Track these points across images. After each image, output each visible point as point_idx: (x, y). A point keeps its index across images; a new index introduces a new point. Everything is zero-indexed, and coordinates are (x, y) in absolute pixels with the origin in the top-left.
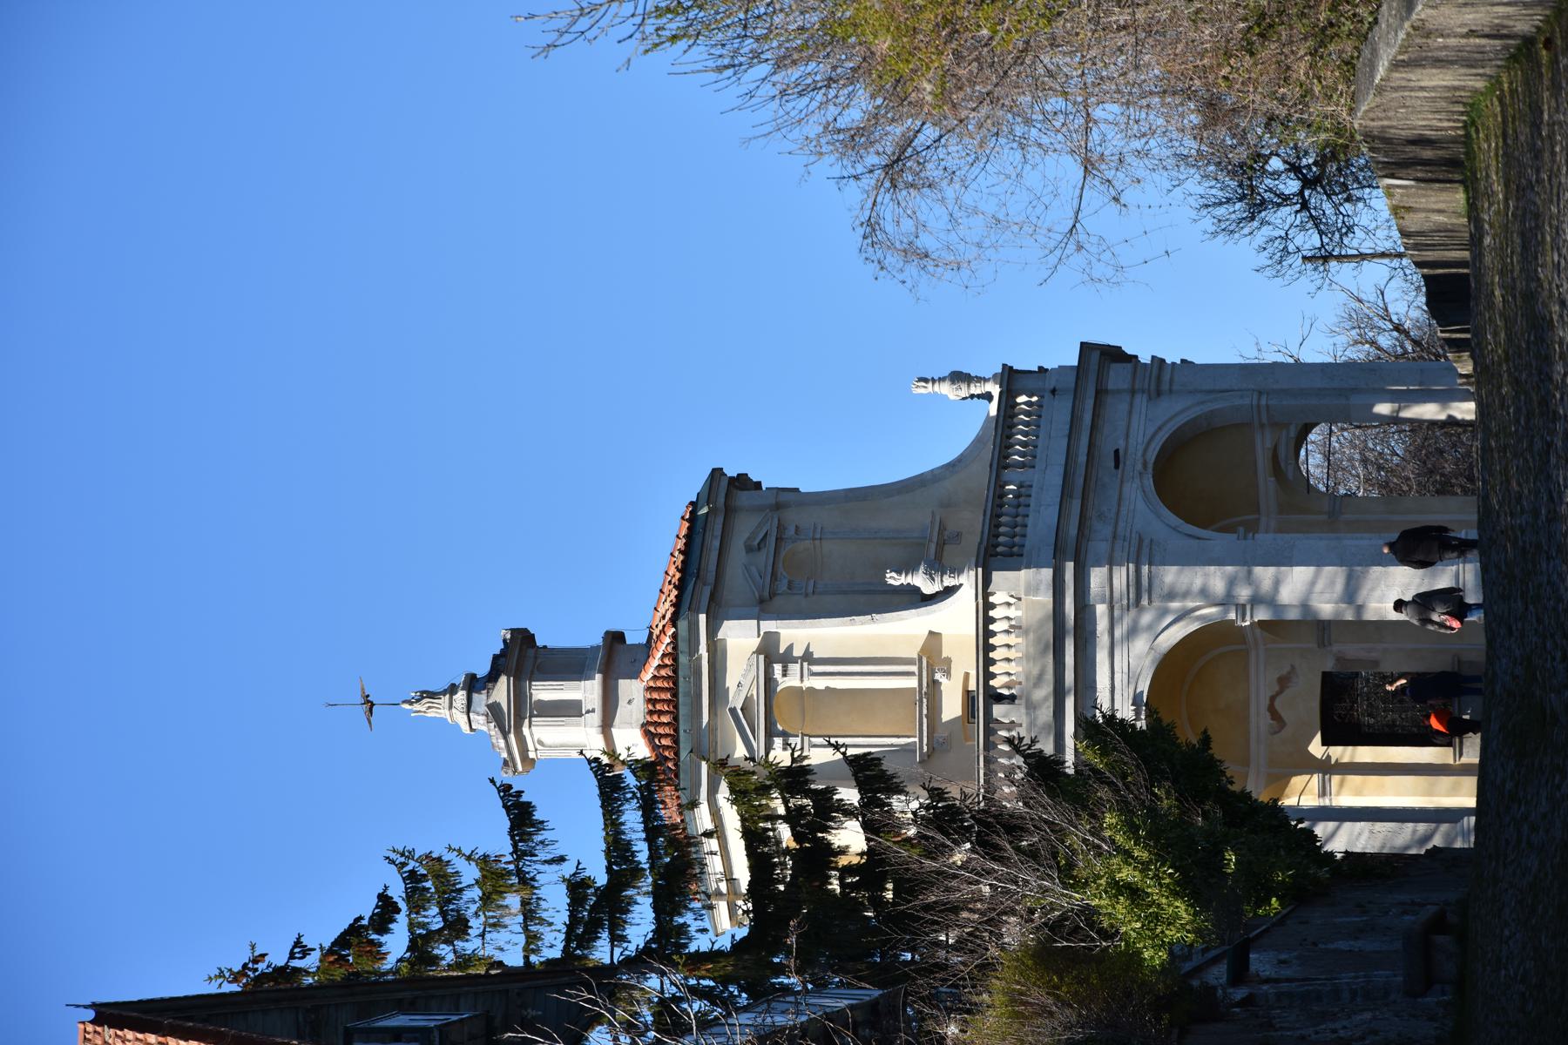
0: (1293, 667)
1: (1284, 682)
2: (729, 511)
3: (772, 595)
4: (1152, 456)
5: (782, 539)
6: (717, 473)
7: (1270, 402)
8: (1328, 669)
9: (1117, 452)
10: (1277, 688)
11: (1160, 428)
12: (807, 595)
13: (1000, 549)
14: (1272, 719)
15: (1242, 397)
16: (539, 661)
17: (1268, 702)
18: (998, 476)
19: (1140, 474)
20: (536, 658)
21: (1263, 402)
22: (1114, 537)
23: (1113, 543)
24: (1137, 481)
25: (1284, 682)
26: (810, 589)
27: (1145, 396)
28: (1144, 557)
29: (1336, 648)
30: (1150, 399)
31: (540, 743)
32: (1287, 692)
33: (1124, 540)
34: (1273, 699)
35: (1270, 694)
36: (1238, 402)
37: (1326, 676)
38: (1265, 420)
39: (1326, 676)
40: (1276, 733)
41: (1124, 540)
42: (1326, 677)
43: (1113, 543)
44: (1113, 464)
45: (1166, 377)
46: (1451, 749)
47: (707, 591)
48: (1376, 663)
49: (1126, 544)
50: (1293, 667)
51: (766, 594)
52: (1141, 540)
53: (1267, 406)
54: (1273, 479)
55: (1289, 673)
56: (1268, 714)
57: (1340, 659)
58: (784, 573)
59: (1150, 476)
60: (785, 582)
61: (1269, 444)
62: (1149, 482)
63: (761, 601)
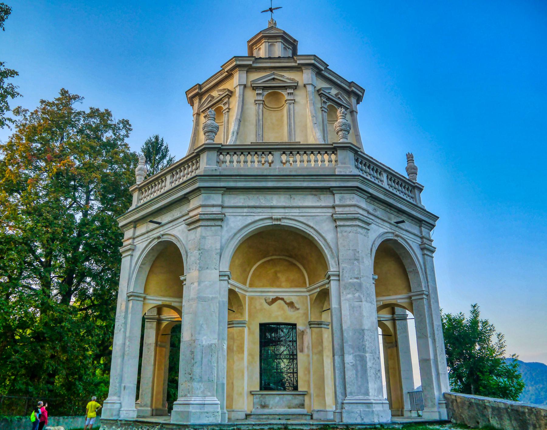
0: (298, 309)
1: (291, 305)
4: (400, 240)
6: (363, 91)
7: (424, 299)
9: (403, 222)
10: (288, 301)
11: (411, 247)
12: (321, 108)
14: (272, 299)
15: (425, 287)
17: (281, 297)
18: (385, 171)
19: (393, 233)
20: (289, 48)
21: (424, 296)
24: (390, 231)
25: (291, 305)
26: (323, 109)
27: (420, 243)
29: (308, 330)
30: (420, 245)
31: (259, 49)
32: (286, 306)
34: (282, 299)
35: (285, 298)
36: (423, 284)
40: (266, 300)
45: (429, 253)
46: (258, 389)
48: (302, 351)
50: (298, 309)
52: (369, 224)
53: (423, 298)
54: (381, 304)
55: (296, 307)
56: (275, 297)
57: (303, 332)
59: (392, 238)
61: (399, 301)
62: (390, 236)
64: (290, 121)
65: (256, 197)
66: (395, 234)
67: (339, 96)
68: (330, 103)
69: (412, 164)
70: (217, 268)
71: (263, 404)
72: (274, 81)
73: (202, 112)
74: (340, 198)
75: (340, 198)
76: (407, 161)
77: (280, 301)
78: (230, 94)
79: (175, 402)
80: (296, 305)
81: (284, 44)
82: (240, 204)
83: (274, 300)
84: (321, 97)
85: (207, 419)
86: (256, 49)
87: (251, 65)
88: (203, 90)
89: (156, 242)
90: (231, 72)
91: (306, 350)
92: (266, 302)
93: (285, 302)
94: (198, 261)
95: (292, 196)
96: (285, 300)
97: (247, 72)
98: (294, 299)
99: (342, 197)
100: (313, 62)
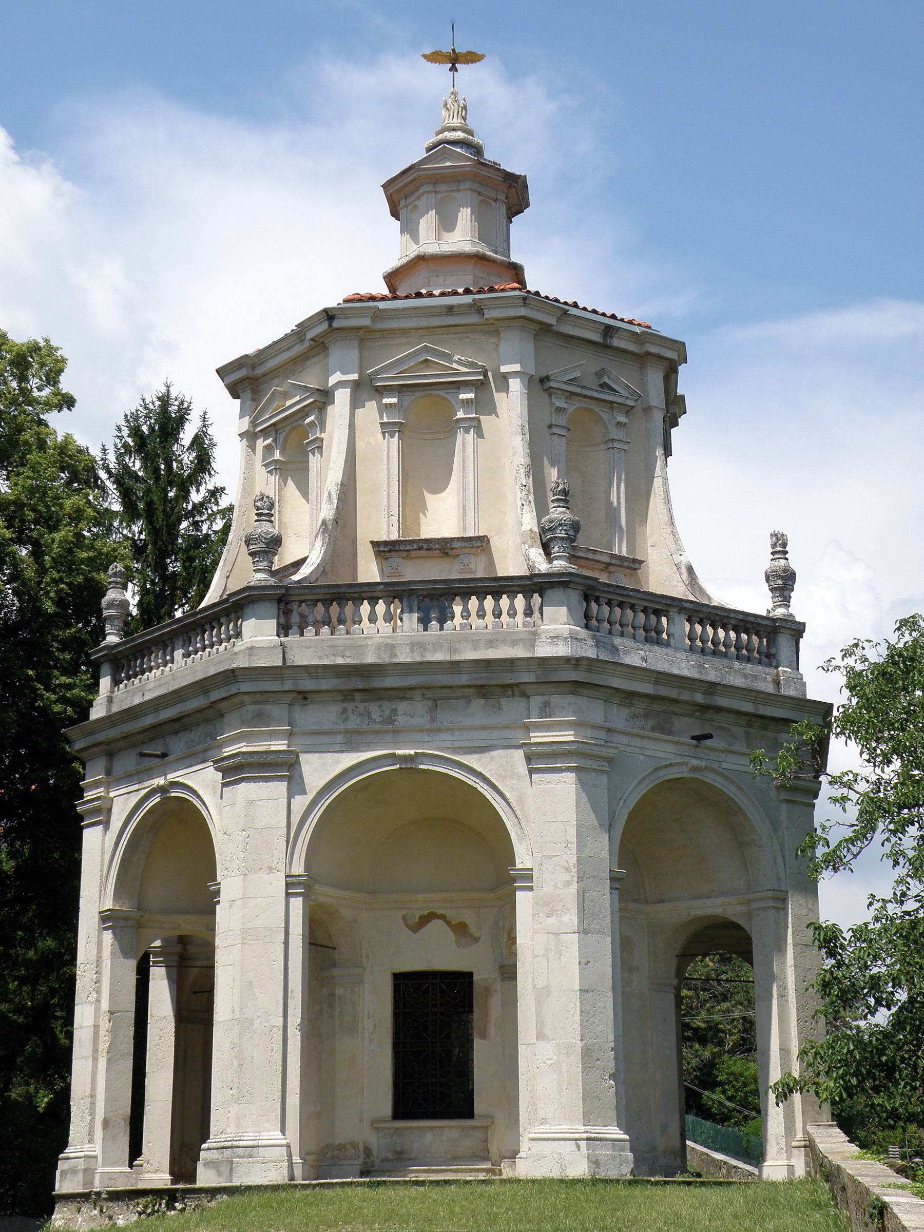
0: (477, 940)
2: (642, 359)
3: (549, 391)
4: (709, 778)
5: (612, 408)
8: (475, 978)
9: (709, 736)
12: (550, 426)
13: (594, 605)
14: (421, 917)
16: (493, 203)
17: (439, 912)
20: (496, 200)
22: (609, 730)
23: (602, 728)
24: (679, 760)
26: (554, 430)
28: (587, 763)
29: (498, 985)
33: (606, 741)
34: (443, 917)
35: (448, 913)
37: (470, 975)
38: (754, 905)
39: (470, 975)
41: (606, 741)
42: (465, 979)
43: (602, 728)
44: (697, 733)
47: (551, 320)
48: (484, 1036)
49: (603, 743)
50: (477, 940)
51: (552, 384)
55: (472, 936)
57: (487, 991)
58: (574, 408)
60: (564, 405)
63: (544, 380)
64: (464, 477)
65: (362, 707)
66: (690, 765)
67: (606, 380)
68: (578, 405)
69: (783, 562)
70: (281, 866)
71: (399, 1150)
72: (428, 366)
73: (261, 431)
74: (541, 705)
75: (541, 705)
76: (773, 553)
77: (436, 924)
78: (325, 397)
79: (204, 1146)
80: (473, 930)
81: (480, 193)
82: (327, 726)
83: (425, 920)
84: (550, 396)
85: (264, 1174)
86: (407, 206)
87: (367, 327)
88: (259, 371)
89: (156, 799)
90: (322, 340)
91: (492, 1030)
92: (407, 925)
93: (448, 923)
94: (242, 855)
95: (439, 702)
96: (448, 919)
97: (362, 340)
98: (468, 917)
99: (547, 704)
100: (522, 312)
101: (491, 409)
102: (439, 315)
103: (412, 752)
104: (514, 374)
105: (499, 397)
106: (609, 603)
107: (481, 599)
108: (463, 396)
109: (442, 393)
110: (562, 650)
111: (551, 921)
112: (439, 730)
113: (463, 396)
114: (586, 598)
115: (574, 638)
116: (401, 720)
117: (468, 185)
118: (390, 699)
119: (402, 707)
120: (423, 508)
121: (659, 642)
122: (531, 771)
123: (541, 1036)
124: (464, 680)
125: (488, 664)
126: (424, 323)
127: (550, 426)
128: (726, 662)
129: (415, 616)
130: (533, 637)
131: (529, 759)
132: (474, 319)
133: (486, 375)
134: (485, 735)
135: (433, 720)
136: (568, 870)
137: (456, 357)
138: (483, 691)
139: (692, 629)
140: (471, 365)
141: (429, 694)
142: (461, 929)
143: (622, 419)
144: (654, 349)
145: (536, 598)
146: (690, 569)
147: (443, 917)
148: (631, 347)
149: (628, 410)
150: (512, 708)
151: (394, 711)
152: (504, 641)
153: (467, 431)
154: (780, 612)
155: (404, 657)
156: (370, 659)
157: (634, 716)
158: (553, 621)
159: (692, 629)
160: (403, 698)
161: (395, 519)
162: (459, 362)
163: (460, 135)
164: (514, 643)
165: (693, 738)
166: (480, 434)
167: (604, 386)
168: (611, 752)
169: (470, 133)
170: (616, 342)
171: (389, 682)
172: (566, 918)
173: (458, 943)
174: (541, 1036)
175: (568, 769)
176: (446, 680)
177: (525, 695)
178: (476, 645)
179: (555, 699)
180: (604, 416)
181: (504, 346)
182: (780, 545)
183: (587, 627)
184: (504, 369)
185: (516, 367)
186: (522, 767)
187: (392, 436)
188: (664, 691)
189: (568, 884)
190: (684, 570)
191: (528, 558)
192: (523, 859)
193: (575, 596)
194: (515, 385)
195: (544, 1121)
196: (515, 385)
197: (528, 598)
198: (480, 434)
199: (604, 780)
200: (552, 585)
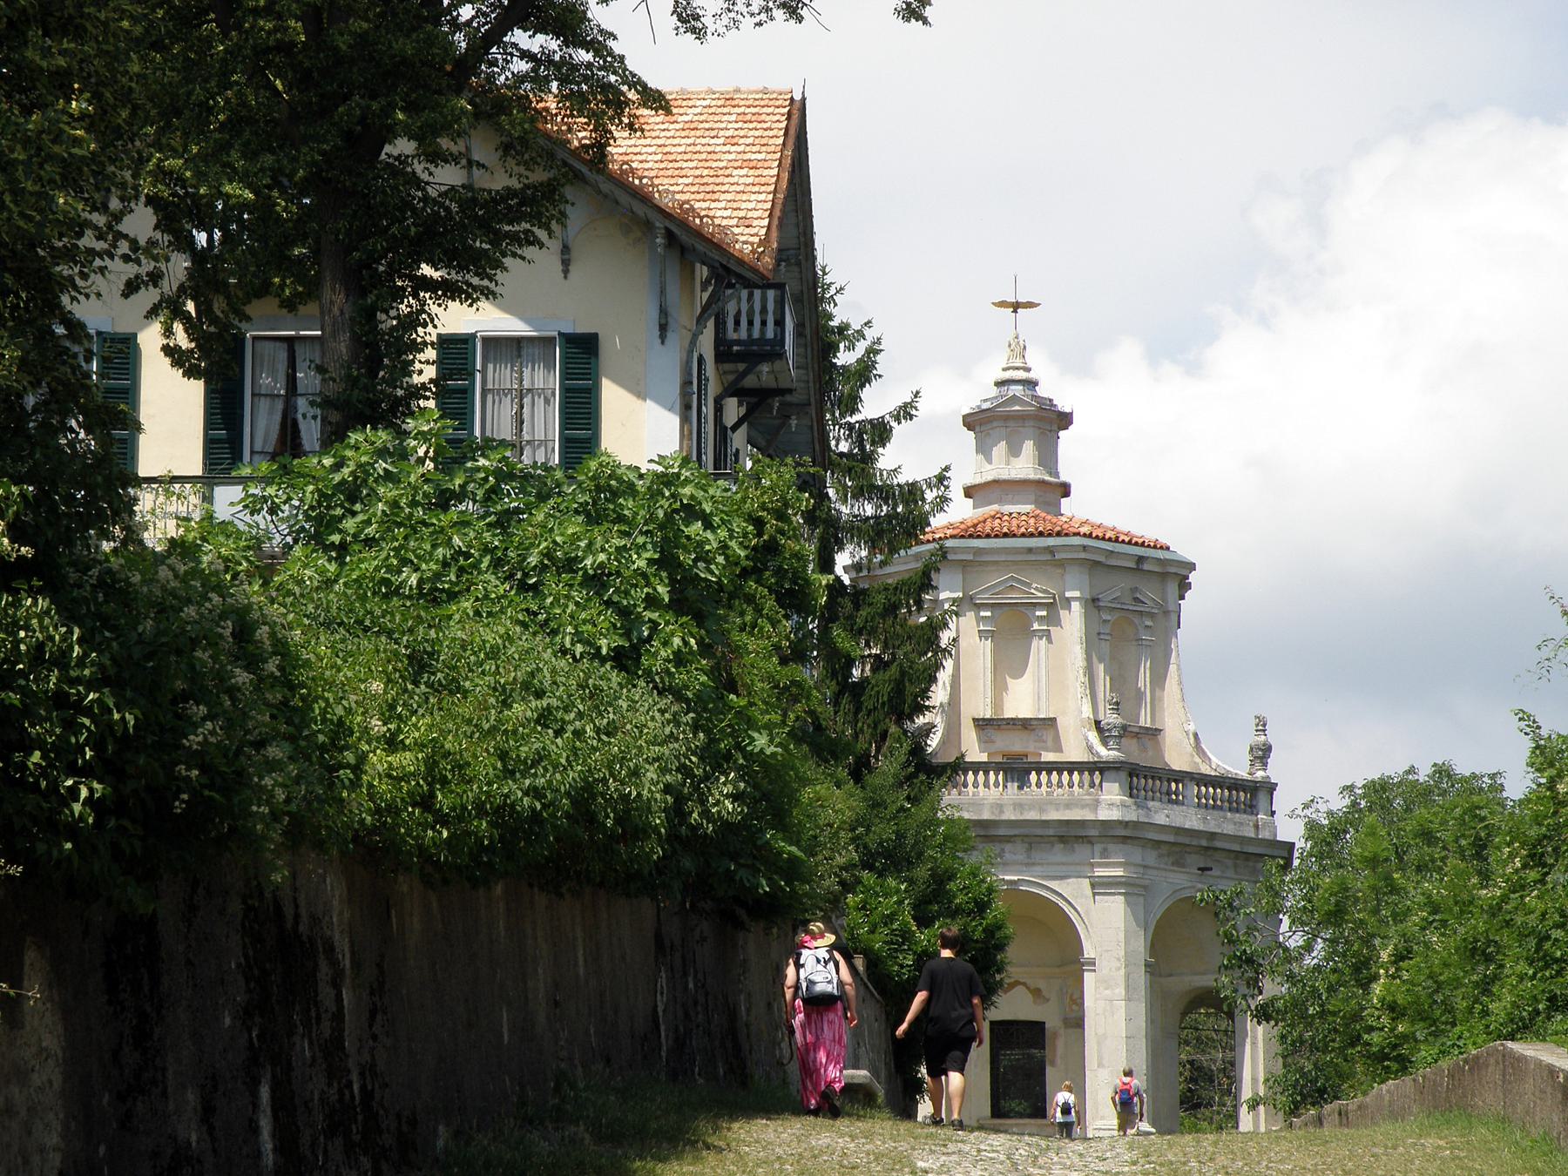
3: (1099, 608)
12: (1099, 634)
24: (1190, 884)
34: (1024, 984)
48: (1053, 1064)
50: (1048, 1000)
57: (1055, 1035)
63: (1095, 600)
77: (1020, 988)
80: (1045, 993)
91: (1059, 1061)
93: (1028, 988)
98: (1042, 985)
101: (1058, 623)
102: (1021, 553)
103: (1016, 878)
104: (1075, 599)
105: (1063, 613)
106: (1145, 777)
107: (1060, 774)
108: (1038, 613)
109: (1022, 609)
110: (1114, 815)
111: (1107, 992)
112: (1033, 864)
113: (1038, 613)
114: (1131, 775)
115: (1123, 805)
116: (1007, 856)
117: (1032, 423)
118: (1000, 842)
119: (1008, 847)
120: (1006, 689)
121: (1176, 802)
122: (1094, 894)
123: (1100, 1065)
124: (1051, 832)
125: (1068, 822)
126: (1010, 558)
127: (1099, 634)
128: (1221, 813)
129: (1016, 784)
130: (1096, 804)
131: (1093, 886)
132: (1049, 557)
133: (1054, 598)
134: (1064, 868)
135: (1029, 857)
136: (1119, 959)
137: (1034, 585)
138: (1062, 839)
139: (1199, 790)
140: (1045, 591)
141: (1026, 839)
142: (1037, 993)
143: (1149, 623)
144: (1173, 570)
145: (1097, 777)
146: (1196, 735)
147: (1024, 984)
148: (1157, 569)
149: (1152, 616)
150: (1082, 851)
151: (1003, 850)
152: (1076, 805)
153: (1041, 638)
154: (1260, 774)
155: (1009, 815)
156: (986, 816)
157: (1160, 856)
158: (1110, 793)
159: (1199, 790)
160: (1009, 842)
161: (989, 700)
162: (1036, 589)
163: (1021, 375)
164: (1083, 807)
165: (1199, 869)
166: (1050, 641)
167: (1137, 600)
168: (1147, 883)
169: (1028, 370)
170: (1146, 567)
171: (1001, 832)
172: (1117, 991)
173: (1035, 1002)
174: (1100, 1065)
175: (1120, 894)
176: (1039, 832)
177: (1092, 844)
178: (1057, 806)
179: (1111, 847)
180: (1136, 621)
181: (1068, 577)
182: (1262, 725)
183: (1131, 796)
184: (1068, 594)
185: (1077, 594)
186: (1089, 892)
187: (987, 639)
188: (1181, 839)
189: (1119, 969)
190: (1191, 736)
191: (1087, 739)
192: (1089, 952)
193: (1123, 775)
194: (1076, 606)
195: (1103, 1118)
196: (1076, 606)
197: (1092, 774)
198: (1050, 641)
199: (1141, 899)
200: (1109, 769)
